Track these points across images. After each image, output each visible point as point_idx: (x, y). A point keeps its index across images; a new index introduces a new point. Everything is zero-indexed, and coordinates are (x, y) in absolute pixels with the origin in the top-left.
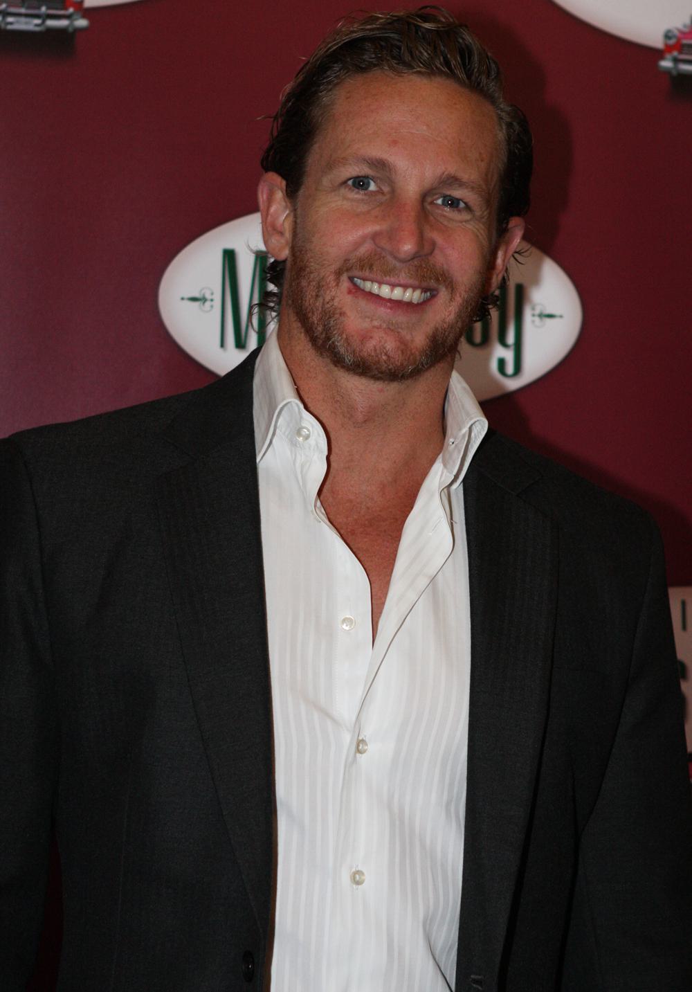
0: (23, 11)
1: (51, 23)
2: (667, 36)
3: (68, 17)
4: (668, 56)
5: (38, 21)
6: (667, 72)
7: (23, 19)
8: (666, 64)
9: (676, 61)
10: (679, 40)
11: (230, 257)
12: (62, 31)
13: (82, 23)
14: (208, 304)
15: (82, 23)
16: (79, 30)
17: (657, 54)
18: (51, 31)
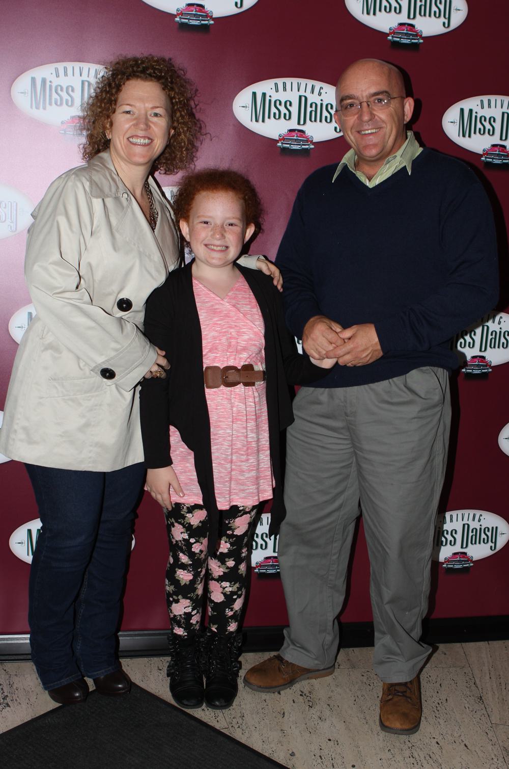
0: (194, 18)
1: (203, 22)
2: (390, 29)
4: (390, 35)
5: (199, 22)
7: (194, 21)
8: (390, 38)
9: (393, 37)
11: (254, 94)
12: (206, 25)
13: (212, 22)
14: (247, 108)
15: (212, 22)
16: (211, 25)
17: (388, 35)
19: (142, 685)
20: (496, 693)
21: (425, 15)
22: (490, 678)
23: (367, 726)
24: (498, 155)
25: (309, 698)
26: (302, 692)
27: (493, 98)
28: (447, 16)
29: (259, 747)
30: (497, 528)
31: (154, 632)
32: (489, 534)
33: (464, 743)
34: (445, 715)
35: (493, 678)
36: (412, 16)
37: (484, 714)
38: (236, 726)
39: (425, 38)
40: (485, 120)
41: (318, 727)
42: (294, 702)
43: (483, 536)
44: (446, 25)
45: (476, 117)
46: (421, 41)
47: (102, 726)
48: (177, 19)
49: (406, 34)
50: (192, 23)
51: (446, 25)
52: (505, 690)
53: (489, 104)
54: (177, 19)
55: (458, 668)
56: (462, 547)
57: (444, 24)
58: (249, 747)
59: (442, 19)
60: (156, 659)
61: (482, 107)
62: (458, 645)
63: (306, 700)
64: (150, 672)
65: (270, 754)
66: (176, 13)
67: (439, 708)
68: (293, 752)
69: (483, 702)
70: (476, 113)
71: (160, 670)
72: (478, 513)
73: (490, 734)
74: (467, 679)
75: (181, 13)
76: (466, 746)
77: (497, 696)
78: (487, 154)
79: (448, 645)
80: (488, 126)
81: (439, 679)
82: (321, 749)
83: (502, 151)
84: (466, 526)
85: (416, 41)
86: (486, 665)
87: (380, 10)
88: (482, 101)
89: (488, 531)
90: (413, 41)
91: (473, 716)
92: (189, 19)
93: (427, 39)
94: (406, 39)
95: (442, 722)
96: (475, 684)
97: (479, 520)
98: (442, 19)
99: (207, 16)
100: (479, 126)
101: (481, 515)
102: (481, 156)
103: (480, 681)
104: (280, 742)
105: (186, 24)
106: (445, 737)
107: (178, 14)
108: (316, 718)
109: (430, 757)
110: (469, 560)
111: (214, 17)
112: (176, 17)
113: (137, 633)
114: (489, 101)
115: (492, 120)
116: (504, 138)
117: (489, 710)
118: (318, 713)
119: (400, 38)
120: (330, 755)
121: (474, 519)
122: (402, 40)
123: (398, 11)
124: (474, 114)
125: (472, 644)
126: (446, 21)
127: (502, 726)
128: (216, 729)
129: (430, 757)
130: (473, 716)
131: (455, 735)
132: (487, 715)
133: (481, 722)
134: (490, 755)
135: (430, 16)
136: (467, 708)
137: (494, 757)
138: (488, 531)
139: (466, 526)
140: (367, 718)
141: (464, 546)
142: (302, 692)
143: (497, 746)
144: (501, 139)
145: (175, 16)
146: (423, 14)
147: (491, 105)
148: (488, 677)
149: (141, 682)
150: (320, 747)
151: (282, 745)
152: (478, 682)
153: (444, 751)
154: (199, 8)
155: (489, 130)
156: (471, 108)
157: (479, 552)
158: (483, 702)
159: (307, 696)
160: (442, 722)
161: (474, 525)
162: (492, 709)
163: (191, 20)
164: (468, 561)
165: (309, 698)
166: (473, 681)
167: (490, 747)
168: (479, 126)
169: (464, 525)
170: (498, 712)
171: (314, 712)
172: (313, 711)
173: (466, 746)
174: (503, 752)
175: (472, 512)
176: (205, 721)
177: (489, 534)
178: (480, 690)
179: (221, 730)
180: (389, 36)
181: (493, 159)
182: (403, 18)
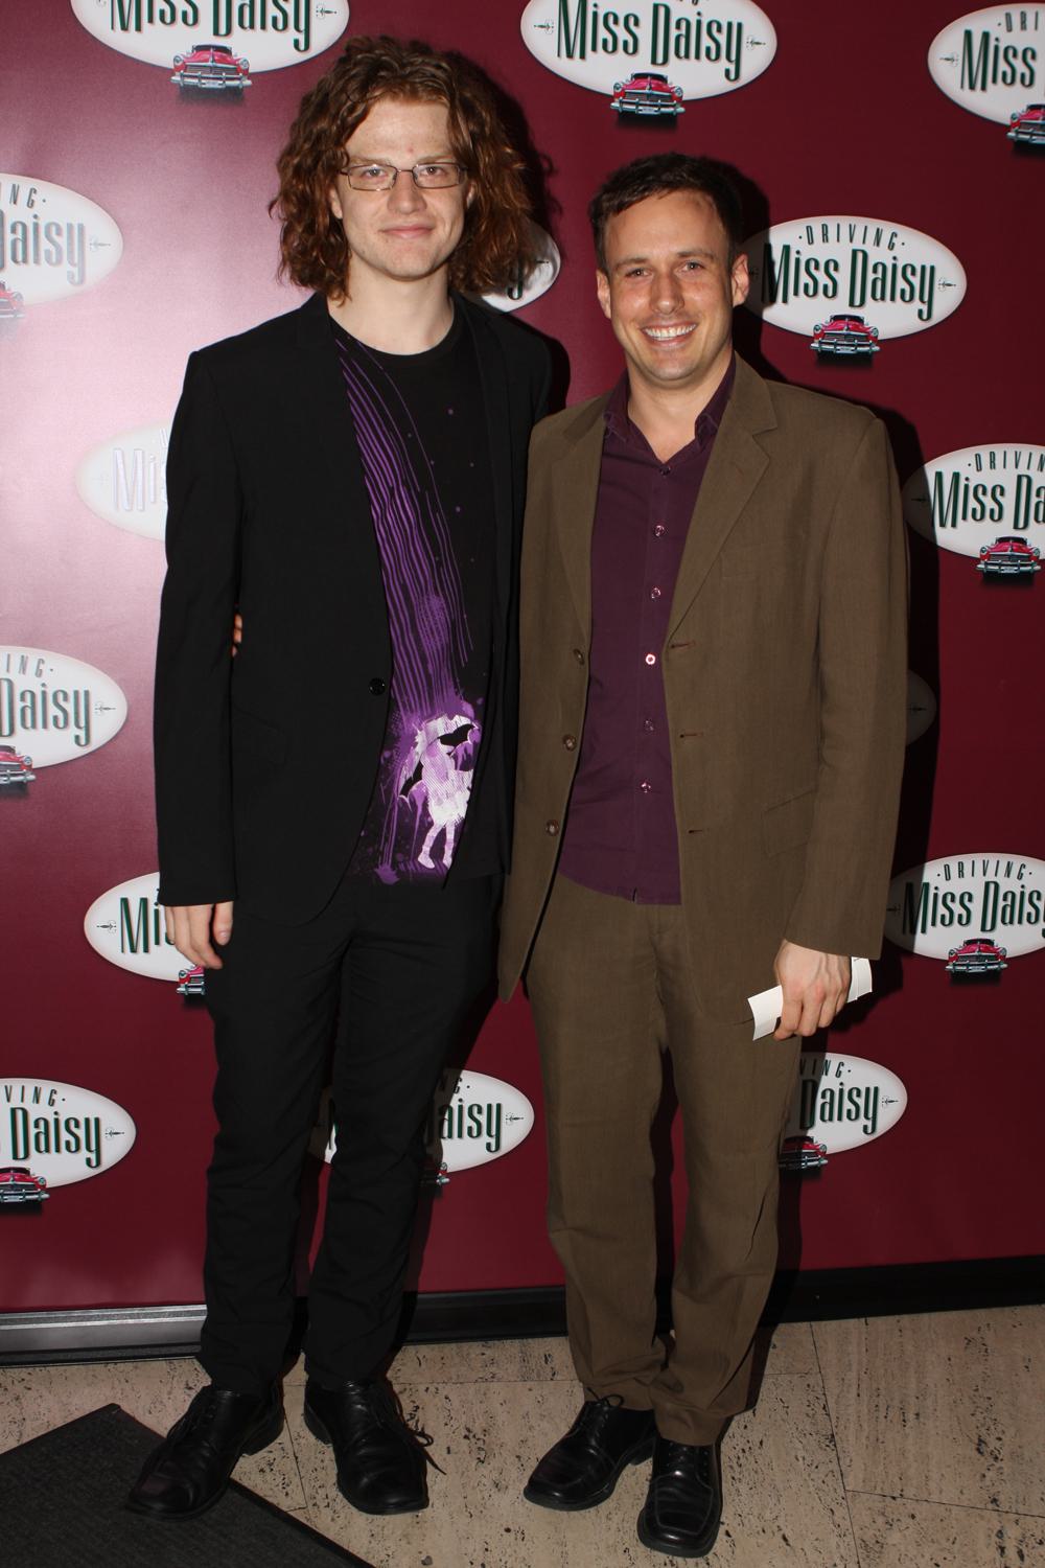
0: (211, 76)
1: (228, 83)
3: (239, 79)
6: (616, 110)
8: (615, 104)
10: (623, 90)
12: (235, 89)
13: (248, 82)
15: (248, 82)
17: (611, 99)
18: (229, 88)
20: (865, 1426)
21: (687, 56)
22: (859, 1395)
24: (846, 336)
25: (480, 1443)
26: (469, 1430)
27: (832, 221)
28: (733, 57)
29: (361, 1547)
30: (876, 1089)
33: (782, 1532)
34: (753, 1473)
35: (865, 1397)
36: (660, 59)
37: (833, 1472)
38: (322, 1505)
39: (688, 104)
40: (817, 268)
42: (449, 1452)
43: (847, 1105)
44: (733, 76)
46: (681, 109)
47: (51, 1508)
48: (176, 78)
49: (649, 96)
50: (207, 86)
51: (733, 76)
52: (884, 1420)
53: (823, 235)
55: (796, 1376)
57: (727, 72)
58: (342, 1549)
59: (724, 64)
61: (811, 241)
63: (474, 1448)
64: (170, 1393)
65: (382, 1561)
67: (742, 1461)
68: (428, 1557)
69: (835, 1445)
70: (798, 252)
71: (190, 1388)
73: (840, 1512)
74: (811, 1398)
75: (183, 67)
76: (785, 1539)
77: (866, 1434)
78: (823, 335)
80: (823, 279)
82: (487, 1550)
83: (856, 329)
85: (671, 110)
86: (855, 1367)
87: (594, 49)
88: (809, 229)
89: (859, 1095)
90: (663, 110)
91: (809, 1475)
93: (692, 105)
94: (650, 105)
95: (743, 1488)
96: (824, 1408)
98: (724, 64)
99: (237, 70)
100: (804, 278)
102: (810, 339)
103: (837, 1403)
104: (406, 1536)
105: (195, 87)
106: (746, 1522)
107: (177, 69)
109: (708, 1564)
111: (250, 71)
112: (174, 75)
114: (825, 228)
115: (832, 265)
116: (857, 302)
117: (845, 1462)
118: (495, 1475)
119: (637, 105)
120: (503, 1561)
122: (640, 108)
123: (631, 50)
124: (793, 256)
126: (732, 68)
127: (867, 1496)
128: (280, 1511)
129: (708, 1564)
130: (809, 1475)
131: (768, 1515)
132: (838, 1475)
133: (824, 1487)
134: (831, 1558)
135: (698, 57)
136: (801, 1459)
137: (838, 1562)
138: (859, 1095)
142: (469, 1430)
143: (849, 1538)
144: (852, 304)
145: (171, 72)
146: (682, 53)
147: (829, 235)
148: (854, 1391)
149: (147, 1414)
150: (486, 1546)
151: (409, 1543)
152: (831, 1405)
153: (737, 1551)
154: (219, 53)
155: (826, 287)
156: (787, 244)
158: (835, 1445)
159: (478, 1439)
162: (851, 1461)
163: (205, 78)
165: (480, 1443)
166: (822, 1402)
167: (834, 1540)
168: (804, 278)
170: (863, 1467)
171: (485, 1473)
172: (484, 1469)
173: (785, 1539)
174: (860, 1551)
178: (834, 1421)
179: (291, 1513)
180: (613, 101)
181: (836, 345)
182: (642, 63)
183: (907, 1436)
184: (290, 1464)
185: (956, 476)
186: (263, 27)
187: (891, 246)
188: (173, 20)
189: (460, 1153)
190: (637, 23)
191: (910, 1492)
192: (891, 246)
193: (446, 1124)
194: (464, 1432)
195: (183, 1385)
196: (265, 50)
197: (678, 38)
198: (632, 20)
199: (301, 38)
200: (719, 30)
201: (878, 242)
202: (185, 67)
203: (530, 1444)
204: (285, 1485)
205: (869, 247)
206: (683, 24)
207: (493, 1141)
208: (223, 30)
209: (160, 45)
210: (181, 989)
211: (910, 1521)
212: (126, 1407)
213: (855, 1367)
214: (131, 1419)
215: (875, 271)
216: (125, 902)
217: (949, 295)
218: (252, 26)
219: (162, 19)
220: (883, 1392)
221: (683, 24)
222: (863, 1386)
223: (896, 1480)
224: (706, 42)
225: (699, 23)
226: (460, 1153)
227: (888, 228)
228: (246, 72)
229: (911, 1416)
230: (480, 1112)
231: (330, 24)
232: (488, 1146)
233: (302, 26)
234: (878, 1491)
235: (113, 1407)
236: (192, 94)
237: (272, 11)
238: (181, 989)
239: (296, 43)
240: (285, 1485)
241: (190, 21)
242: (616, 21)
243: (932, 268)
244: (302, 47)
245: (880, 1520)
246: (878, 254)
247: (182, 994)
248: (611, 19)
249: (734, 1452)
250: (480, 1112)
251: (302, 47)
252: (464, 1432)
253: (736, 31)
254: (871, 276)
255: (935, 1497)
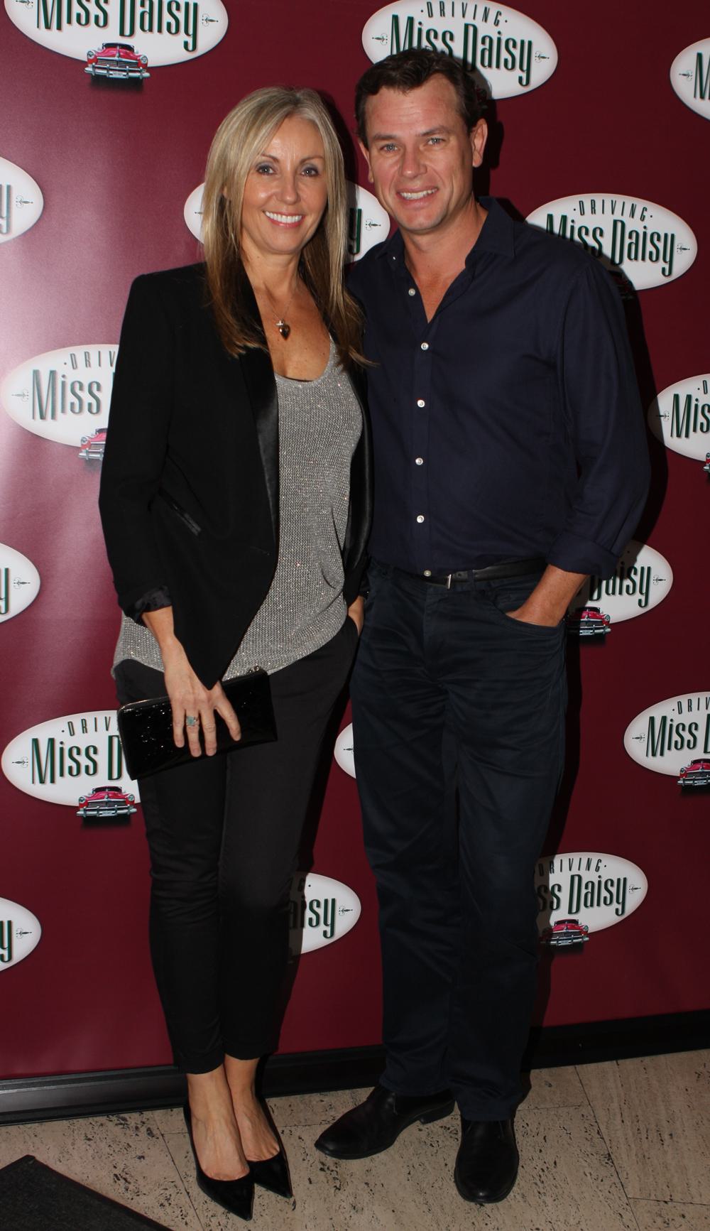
12: (137, 79)
13: (147, 75)
15: (147, 75)
19: (60, 1168)
23: (430, 1216)
25: (334, 1174)
27: (598, 198)
31: (78, 1076)
32: (614, 890)
41: (351, 1222)
45: (572, 228)
48: (89, 69)
54: (89, 69)
56: (570, 912)
57: (520, 79)
59: (518, 72)
60: (81, 1123)
61: (582, 213)
62: (570, 1069)
63: (330, 1178)
64: (73, 1144)
66: (85, 60)
67: (543, 1178)
72: (595, 857)
77: (634, 1152)
79: (555, 1070)
81: (542, 1129)
84: (576, 879)
86: (616, 1100)
88: (581, 203)
92: (108, 70)
95: (549, 1200)
97: (597, 869)
98: (518, 72)
99: (138, 64)
101: (600, 861)
107: (90, 61)
108: (348, 1207)
110: (583, 931)
113: (48, 1079)
114: (593, 202)
117: (623, 1176)
118: (351, 1199)
121: (588, 868)
124: (569, 224)
125: (592, 1066)
126: (524, 76)
127: (643, 1202)
131: (572, 1221)
135: (498, 66)
139: (576, 879)
140: (431, 1201)
141: (574, 910)
145: (85, 64)
148: (619, 1118)
152: (603, 1130)
157: (597, 918)
160: (549, 1200)
161: (588, 876)
164: (580, 933)
165: (334, 1174)
169: (573, 877)
172: (342, 1195)
175: (585, 856)
176: (165, 1224)
177: (614, 890)
183: (665, 1152)
184: (184, 1199)
185: (689, 397)
186: (160, 31)
187: (643, 218)
188: (88, 21)
189: (312, 939)
190: (452, 38)
191: (677, 1197)
192: (643, 218)
193: (292, 916)
194: (320, 1166)
195: (83, 1137)
196: (161, 49)
197: (483, 51)
198: (448, 36)
199: (190, 40)
200: (514, 46)
201: (632, 215)
202: (96, 60)
203: (374, 1172)
204: (183, 1216)
205: (626, 218)
206: (487, 41)
207: (328, 929)
208: (127, 32)
209: (77, 42)
210: (81, 812)
211: (681, 1219)
212: (39, 1158)
213: (616, 1100)
214: (45, 1168)
215: (630, 237)
216: (36, 742)
217: (684, 260)
218: (151, 30)
219: (79, 21)
220: (641, 1118)
221: (487, 41)
222: (625, 1114)
223: (665, 1187)
224: (504, 55)
225: (499, 40)
226: (312, 939)
227: (640, 204)
228: (145, 66)
229: (666, 1137)
230: (318, 906)
231: (212, 32)
232: (325, 933)
233: (191, 31)
234: (653, 1197)
235: (28, 1158)
236: (99, 81)
237: (167, 18)
238: (81, 812)
239: (186, 44)
240: (183, 1216)
241: (101, 23)
242: (436, 37)
243: (673, 236)
244: (190, 47)
245: (659, 1220)
246: (633, 224)
247: (81, 816)
248: (432, 34)
249: (534, 1173)
250: (318, 906)
251: (190, 47)
252: (320, 1166)
253: (527, 47)
254: (627, 241)
255: (697, 1200)
